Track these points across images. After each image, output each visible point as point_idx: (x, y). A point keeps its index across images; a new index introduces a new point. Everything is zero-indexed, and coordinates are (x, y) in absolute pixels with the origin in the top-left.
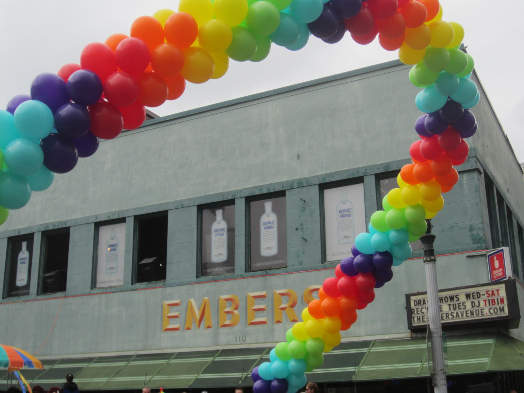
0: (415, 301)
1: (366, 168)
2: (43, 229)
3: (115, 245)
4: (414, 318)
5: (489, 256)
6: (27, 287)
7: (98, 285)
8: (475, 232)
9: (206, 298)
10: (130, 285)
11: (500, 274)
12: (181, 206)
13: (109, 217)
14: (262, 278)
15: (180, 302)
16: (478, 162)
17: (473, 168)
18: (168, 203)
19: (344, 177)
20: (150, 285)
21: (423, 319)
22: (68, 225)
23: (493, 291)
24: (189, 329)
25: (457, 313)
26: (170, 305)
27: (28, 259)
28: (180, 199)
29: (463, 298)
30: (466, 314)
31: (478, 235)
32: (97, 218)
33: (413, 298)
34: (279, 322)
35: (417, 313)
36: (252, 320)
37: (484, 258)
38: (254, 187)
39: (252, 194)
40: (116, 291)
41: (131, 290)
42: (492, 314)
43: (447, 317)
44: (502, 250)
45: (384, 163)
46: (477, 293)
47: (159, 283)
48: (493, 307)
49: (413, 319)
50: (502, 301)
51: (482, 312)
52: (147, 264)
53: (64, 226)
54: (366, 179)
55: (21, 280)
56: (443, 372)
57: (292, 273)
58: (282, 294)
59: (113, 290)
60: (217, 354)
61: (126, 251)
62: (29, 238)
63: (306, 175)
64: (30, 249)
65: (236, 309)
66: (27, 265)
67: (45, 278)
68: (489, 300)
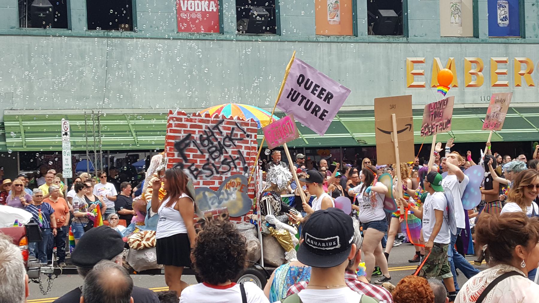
9: (452, 58)
15: (424, 60)
34: (518, 85)
36: (495, 83)
41: (369, 43)
47: (403, 39)
58: (521, 62)
65: (480, 71)
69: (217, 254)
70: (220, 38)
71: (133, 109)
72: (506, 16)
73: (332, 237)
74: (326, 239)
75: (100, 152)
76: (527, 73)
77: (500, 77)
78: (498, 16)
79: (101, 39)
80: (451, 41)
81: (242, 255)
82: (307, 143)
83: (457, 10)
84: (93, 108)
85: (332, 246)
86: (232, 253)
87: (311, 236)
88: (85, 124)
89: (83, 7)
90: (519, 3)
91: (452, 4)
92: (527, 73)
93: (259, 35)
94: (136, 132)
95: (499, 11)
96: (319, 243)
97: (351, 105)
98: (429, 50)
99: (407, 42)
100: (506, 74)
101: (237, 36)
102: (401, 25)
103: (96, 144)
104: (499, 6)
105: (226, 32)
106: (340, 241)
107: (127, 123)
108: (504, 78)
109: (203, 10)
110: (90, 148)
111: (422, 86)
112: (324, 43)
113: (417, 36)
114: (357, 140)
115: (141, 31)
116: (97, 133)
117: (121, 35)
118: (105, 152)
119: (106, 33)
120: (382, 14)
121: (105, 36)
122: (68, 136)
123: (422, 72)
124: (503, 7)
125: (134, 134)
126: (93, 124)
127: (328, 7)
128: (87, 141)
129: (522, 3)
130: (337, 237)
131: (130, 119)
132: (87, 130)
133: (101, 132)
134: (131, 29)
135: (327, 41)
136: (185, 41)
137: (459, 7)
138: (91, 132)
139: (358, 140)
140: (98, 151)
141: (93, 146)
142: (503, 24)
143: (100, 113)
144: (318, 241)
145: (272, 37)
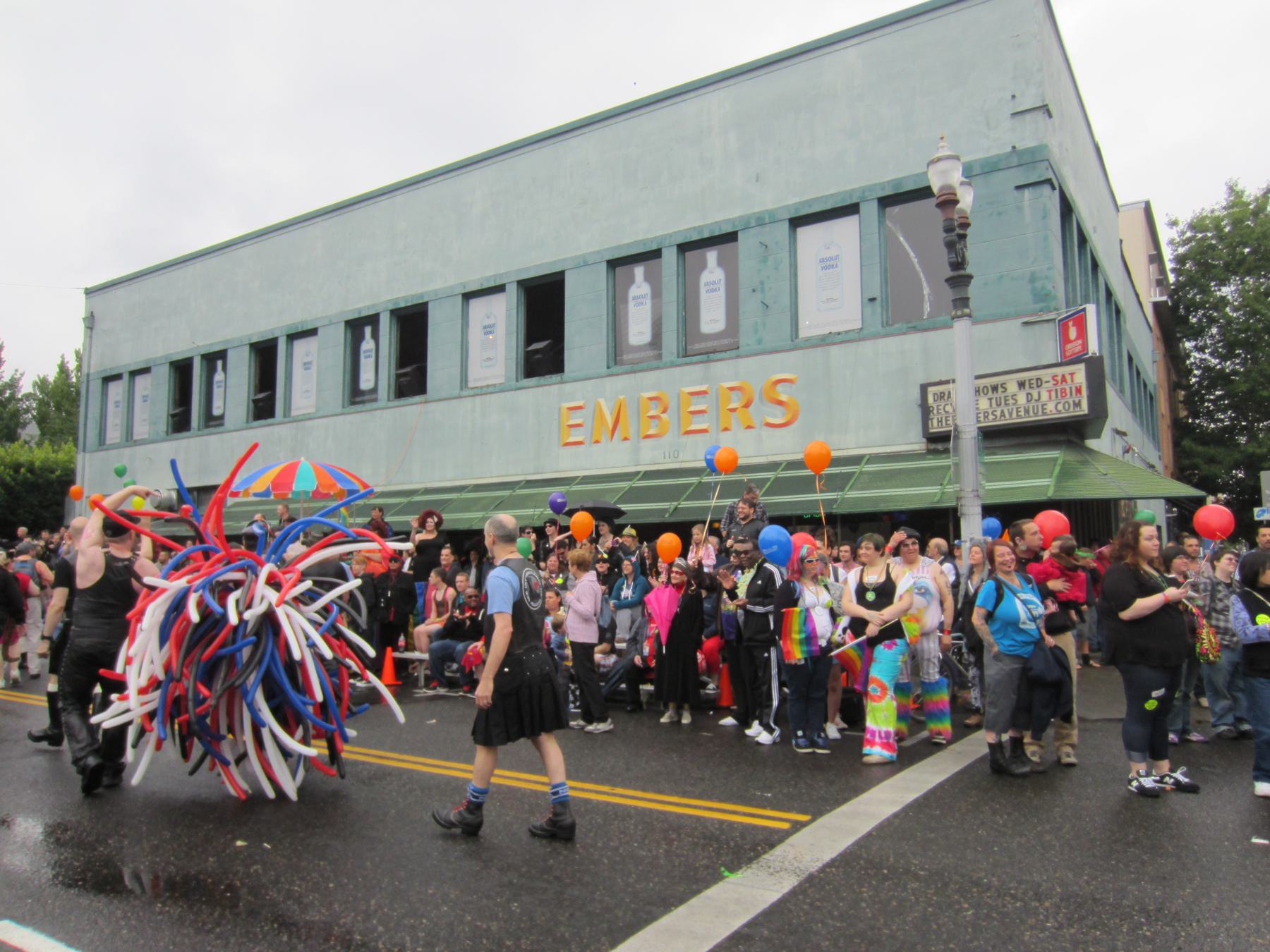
0: (934, 394)
1: (864, 190)
2: (391, 307)
3: (493, 326)
4: (932, 419)
5: (1060, 321)
6: (374, 390)
7: (471, 385)
8: (1038, 285)
10: (513, 383)
11: (1078, 349)
12: (584, 263)
13: (482, 285)
14: (702, 365)
16: (1050, 169)
17: (1042, 179)
18: (565, 260)
19: (829, 206)
20: (542, 380)
21: (946, 421)
22: (425, 300)
23: (1063, 376)
24: (597, 442)
25: (1002, 411)
26: (570, 409)
27: (374, 351)
28: (582, 253)
29: (1012, 388)
30: (1018, 412)
31: (1043, 288)
32: (464, 287)
33: (931, 390)
34: (726, 429)
35: (938, 412)
37: (1051, 325)
38: (690, 229)
39: (687, 240)
42: (1059, 412)
43: (986, 417)
44: (1084, 310)
45: (892, 180)
46: (1037, 379)
47: (555, 378)
48: (1063, 401)
49: (930, 422)
50: (1079, 391)
51: (1043, 409)
52: (537, 351)
53: (421, 302)
54: (863, 208)
55: (366, 382)
56: (976, 493)
57: (747, 356)
58: (732, 389)
59: (490, 390)
60: (638, 478)
61: (508, 334)
62: (373, 320)
63: (770, 206)
64: (375, 336)
65: (664, 412)
66: (373, 359)
67: (398, 376)
68: (1056, 390)
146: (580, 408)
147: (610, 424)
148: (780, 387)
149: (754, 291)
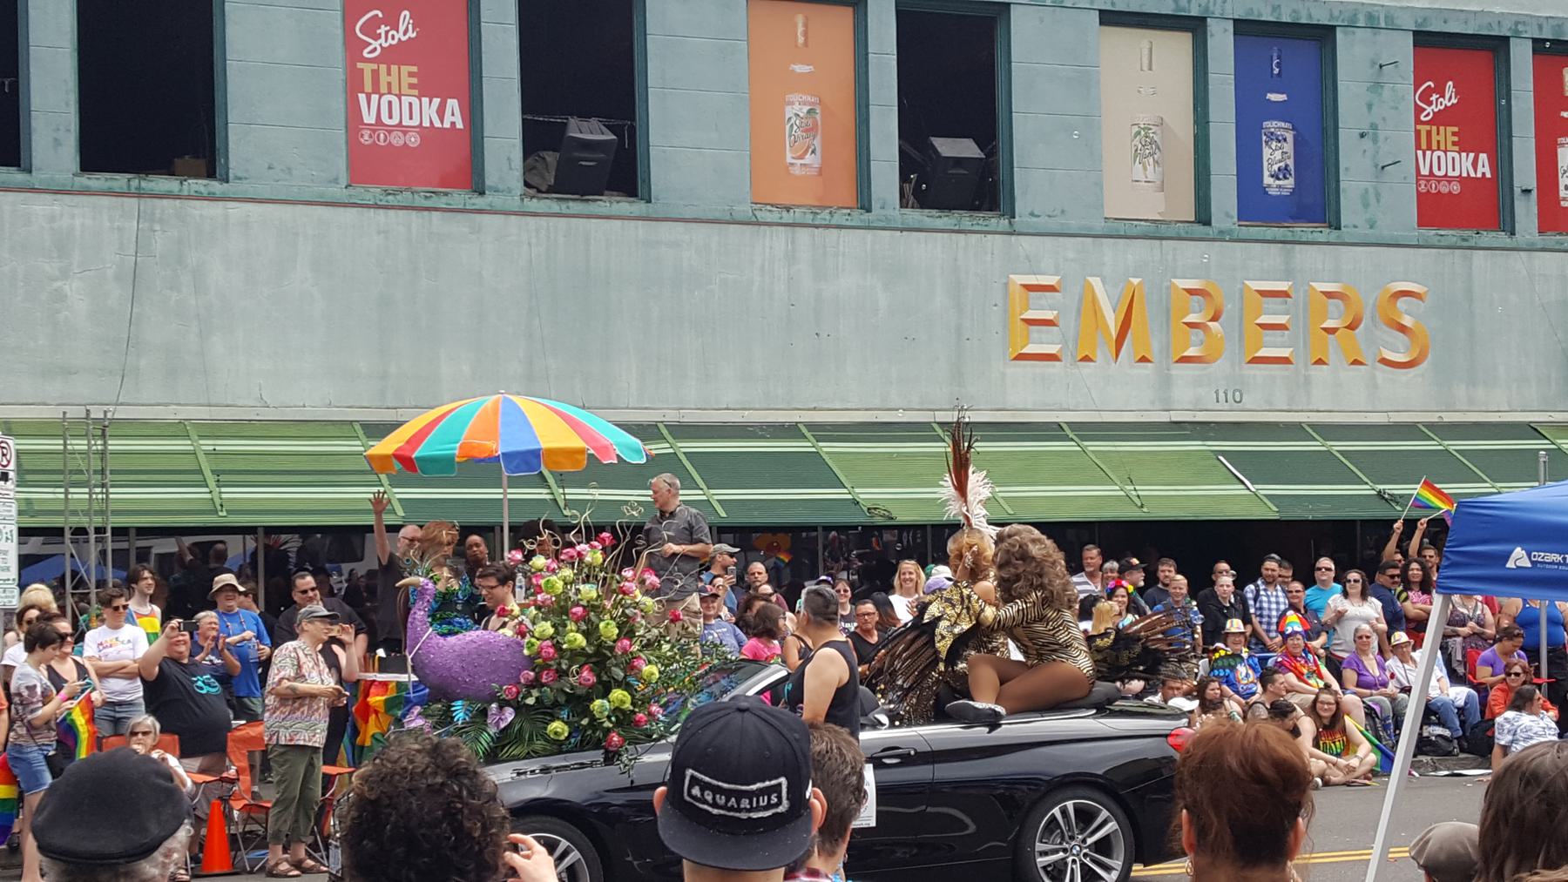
1: (1519, 21)
9: (1136, 281)
14: (1280, 245)
15: (1059, 282)
24: (1086, 359)
36: (1256, 352)
40: (848, 223)
41: (902, 230)
47: (997, 222)
58: (1329, 295)
65: (1215, 319)
69: (423, 831)
70: (474, 204)
71: (210, 406)
72: (1287, 166)
73: (770, 780)
74: (754, 787)
75: (105, 533)
76: (1346, 327)
77: (1269, 335)
78: (1265, 164)
79: (120, 199)
80: (1135, 232)
81: (494, 831)
82: (724, 515)
83: (1149, 144)
84: (89, 401)
85: (769, 806)
86: (467, 824)
87: (707, 779)
88: (62, 447)
89: (67, 105)
90: (1324, 130)
91: (1136, 129)
92: (1346, 327)
93: (589, 200)
94: (215, 472)
95: (1266, 152)
96: (733, 799)
97: (849, 406)
98: (1071, 255)
99: (1008, 229)
100: (1287, 329)
101: (522, 200)
102: (995, 184)
103: (96, 507)
104: (1268, 137)
105: (491, 188)
106: (788, 792)
107: (192, 448)
108: (1279, 339)
109: (426, 124)
110: (76, 521)
111: (1052, 357)
112: (774, 228)
113: (1039, 216)
114: (865, 509)
115: (240, 179)
116: (99, 477)
117: (181, 190)
118: (119, 532)
119: (135, 183)
120: (939, 150)
121: (133, 191)
122: (9, 483)
123: (1051, 317)
124: (1280, 141)
125: (211, 480)
126: (86, 447)
127: (788, 127)
128: (66, 498)
129: (1330, 132)
130: (783, 780)
131: (201, 437)
132: (71, 466)
133: (112, 472)
134: (211, 174)
135: (783, 221)
136: (372, 210)
137: (1155, 138)
138: (81, 472)
139: (869, 509)
140: (98, 530)
141: (86, 513)
142: (1279, 187)
143: (109, 415)
144: (729, 794)
145: (624, 206)
146: (1050, 289)
147: (1114, 333)
148: (1402, 303)
149: (1362, 136)
